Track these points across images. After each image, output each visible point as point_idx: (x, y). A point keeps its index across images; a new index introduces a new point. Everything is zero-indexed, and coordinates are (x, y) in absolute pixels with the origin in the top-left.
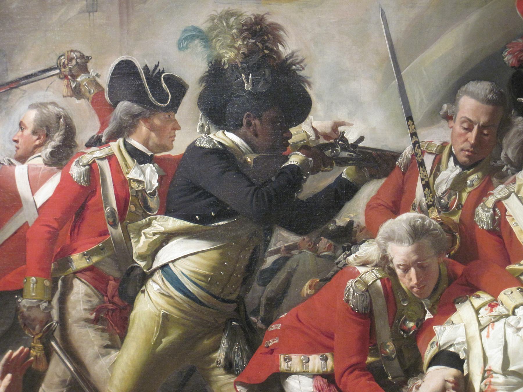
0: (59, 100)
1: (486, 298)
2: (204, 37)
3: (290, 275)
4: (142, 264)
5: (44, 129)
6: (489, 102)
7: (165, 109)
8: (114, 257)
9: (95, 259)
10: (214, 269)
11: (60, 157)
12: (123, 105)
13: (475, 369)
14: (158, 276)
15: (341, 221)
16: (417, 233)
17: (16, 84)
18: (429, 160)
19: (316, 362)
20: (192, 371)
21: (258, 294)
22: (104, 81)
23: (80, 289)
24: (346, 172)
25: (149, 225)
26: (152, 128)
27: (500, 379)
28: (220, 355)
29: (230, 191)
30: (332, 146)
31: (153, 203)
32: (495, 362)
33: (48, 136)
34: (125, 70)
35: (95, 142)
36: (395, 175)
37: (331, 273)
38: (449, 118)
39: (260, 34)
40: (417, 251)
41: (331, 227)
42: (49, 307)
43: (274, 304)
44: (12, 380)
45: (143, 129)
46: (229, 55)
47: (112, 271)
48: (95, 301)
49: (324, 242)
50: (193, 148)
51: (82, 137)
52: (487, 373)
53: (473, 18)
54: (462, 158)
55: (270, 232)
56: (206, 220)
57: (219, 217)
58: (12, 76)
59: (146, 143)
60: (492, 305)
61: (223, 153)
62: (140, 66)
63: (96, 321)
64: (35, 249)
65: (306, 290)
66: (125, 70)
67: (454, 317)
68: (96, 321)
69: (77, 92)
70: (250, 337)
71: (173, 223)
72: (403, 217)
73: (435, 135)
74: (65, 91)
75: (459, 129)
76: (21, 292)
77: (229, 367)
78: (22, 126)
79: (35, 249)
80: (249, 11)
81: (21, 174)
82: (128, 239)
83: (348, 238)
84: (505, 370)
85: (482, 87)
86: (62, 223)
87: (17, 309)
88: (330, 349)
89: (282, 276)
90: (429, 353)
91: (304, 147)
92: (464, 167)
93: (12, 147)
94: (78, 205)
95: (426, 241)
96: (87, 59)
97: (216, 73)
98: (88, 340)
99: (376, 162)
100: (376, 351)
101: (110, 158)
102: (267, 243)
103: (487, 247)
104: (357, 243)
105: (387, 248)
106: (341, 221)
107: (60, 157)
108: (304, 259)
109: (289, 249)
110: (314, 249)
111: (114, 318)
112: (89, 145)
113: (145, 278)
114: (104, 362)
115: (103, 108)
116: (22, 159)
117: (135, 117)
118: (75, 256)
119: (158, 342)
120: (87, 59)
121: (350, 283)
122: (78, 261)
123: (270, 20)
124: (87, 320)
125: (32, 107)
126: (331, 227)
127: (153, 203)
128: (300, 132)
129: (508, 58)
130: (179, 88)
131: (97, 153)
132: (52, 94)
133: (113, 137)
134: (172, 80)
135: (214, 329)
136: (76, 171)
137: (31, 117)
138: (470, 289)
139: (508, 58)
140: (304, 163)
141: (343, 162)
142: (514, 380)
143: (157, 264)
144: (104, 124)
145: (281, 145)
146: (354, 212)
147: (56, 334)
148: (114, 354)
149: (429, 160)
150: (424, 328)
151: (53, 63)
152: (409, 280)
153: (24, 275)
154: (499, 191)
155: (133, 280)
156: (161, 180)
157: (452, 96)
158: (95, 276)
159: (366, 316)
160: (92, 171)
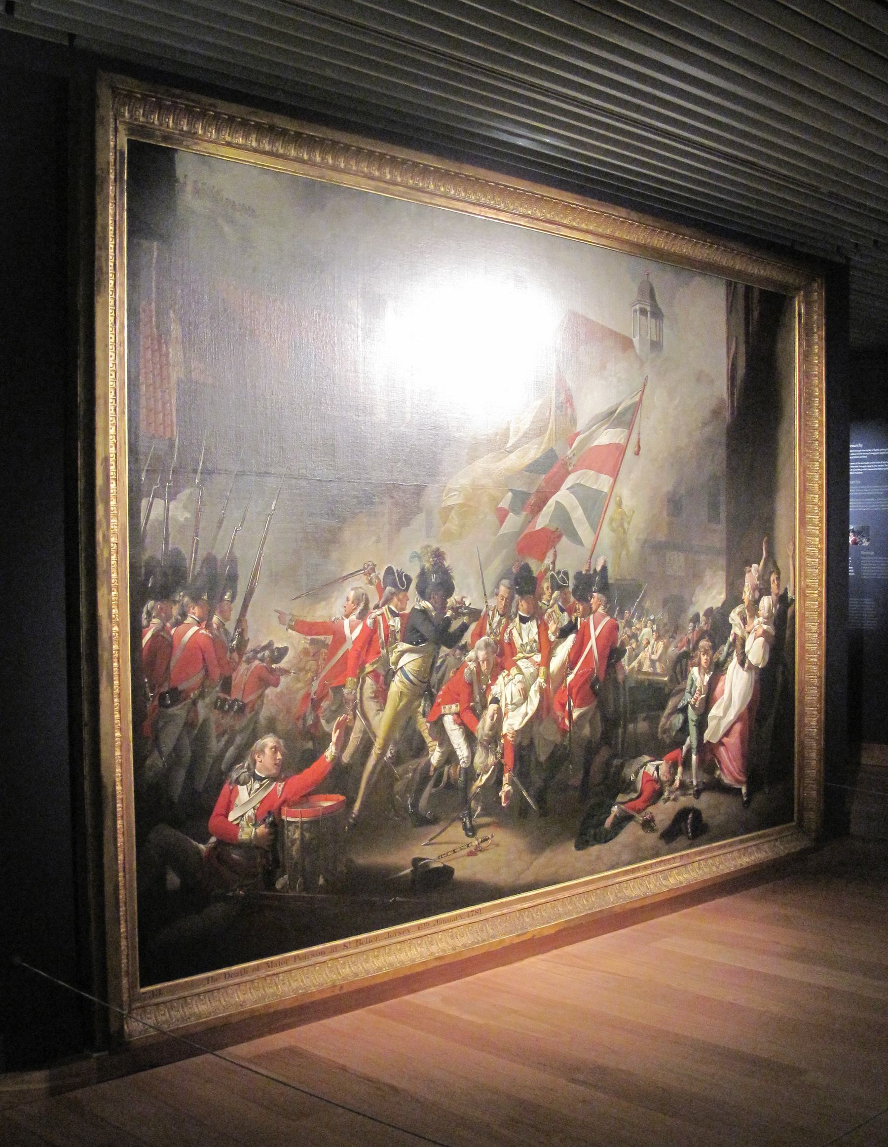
0: (363, 585)
1: (506, 672)
2: (420, 558)
3: (446, 668)
4: (393, 667)
5: (357, 601)
6: (509, 588)
7: (404, 591)
8: (383, 665)
9: (375, 666)
10: (420, 667)
11: (363, 616)
12: (388, 588)
13: (503, 703)
14: (399, 673)
15: (463, 642)
16: (487, 645)
17: (346, 578)
18: (491, 613)
19: (454, 708)
20: (410, 718)
21: (435, 678)
22: (381, 577)
23: (369, 681)
24: (465, 619)
25: (396, 647)
26: (399, 600)
27: (510, 707)
28: (421, 709)
29: (426, 630)
30: (461, 607)
31: (398, 636)
32: (509, 701)
33: (358, 604)
34: (389, 571)
35: (377, 607)
36: (481, 620)
37: (460, 666)
38: (497, 595)
39: (438, 555)
40: (487, 653)
41: (460, 644)
42: (356, 693)
43: (440, 682)
44: (340, 733)
45: (395, 599)
46: (427, 565)
47: (382, 672)
48: (375, 687)
49: (458, 651)
50: (413, 609)
51: (371, 605)
52: (506, 704)
53: (504, 551)
54: (501, 613)
55: (439, 648)
56: (418, 644)
57: (422, 643)
58: (345, 574)
59: (396, 607)
60: (508, 675)
61: (424, 611)
62: (395, 570)
63: (375, 697)
64: (351, 662)
65: (451, 674)
66: (389, 571)
67: (497, 682)
68: (375, 697)
69: (371, 582)
70: (432, 697)
71: (406, 646)
72: (483, 638)
73: (492, 602)
74: (366, 581)
75: (500, 598)
76: (344, 686)
77: (424, 715)
78: (348, 599)
79: (351, 662)
80: (435, 546)
81: (346, 623)
82: (388, 655)
83: (465, 649)
84: (512, 704)
85: (505, 582)
86: (362, 648)
87: (343, 695)
88: (458, 701)
89: (443, 668)
90: (490, 698)
91: (452, 609)
92: (501, 616)
93: (343, 610)
94: (369, 638)
95: (490, 649)
96: (375, 566)
97: (423, 574)
98: (371, 706)
99: (475, 614)
100: (473, 700)
101: (382, 614)
102: (438, 653)
103: (507, 650)
104: (468, 651)
105: (477, 654)
106: (463, 642)
107: (363, 616)
108: (451, 660)
109: (446, 655)
110: (454, 655)
111: (381, 695)
112: (374, 609)
113: (394, 673)
114: (377, 718)
115: (381, 591)
116: (347, 616)
117: (393, 594)
118: (367, 665)
119: (398, 706)
120: (375, 566)
121: (466, 670)
122: (369, 668)
123: (442, 550)
124: (371, 698)
125: (352, 589)
126: (460, 644)
127: (398, 636)
128: (451, 601)
129: (514, 570)
130: (409, 580)
131: (378, 612)
132: (360, 583)
133: (384, 605)
134: (406, 576)
135: (421, 696)
136: (369, 622)
137: (352, 594)
138: (503, 669)
139: (514, 570)
140: (452, 615)
141: (464, 614)
142: (514, 706)
143: (399, 666)
144: (380, 598)
145: (443, 608)
146: (467, 638)
147: (358, 705)
148: (381, 713)
149: (491, 613)
150: (489, 687)
151: (362, 568)
152: (484, 667)
153: (346, 676)
154: (511, 626)
155: (390, 675)
156: (401, 625)
157: (498, 587)
158: (375, 674)
159: (471, 684)
160: (375, 621)
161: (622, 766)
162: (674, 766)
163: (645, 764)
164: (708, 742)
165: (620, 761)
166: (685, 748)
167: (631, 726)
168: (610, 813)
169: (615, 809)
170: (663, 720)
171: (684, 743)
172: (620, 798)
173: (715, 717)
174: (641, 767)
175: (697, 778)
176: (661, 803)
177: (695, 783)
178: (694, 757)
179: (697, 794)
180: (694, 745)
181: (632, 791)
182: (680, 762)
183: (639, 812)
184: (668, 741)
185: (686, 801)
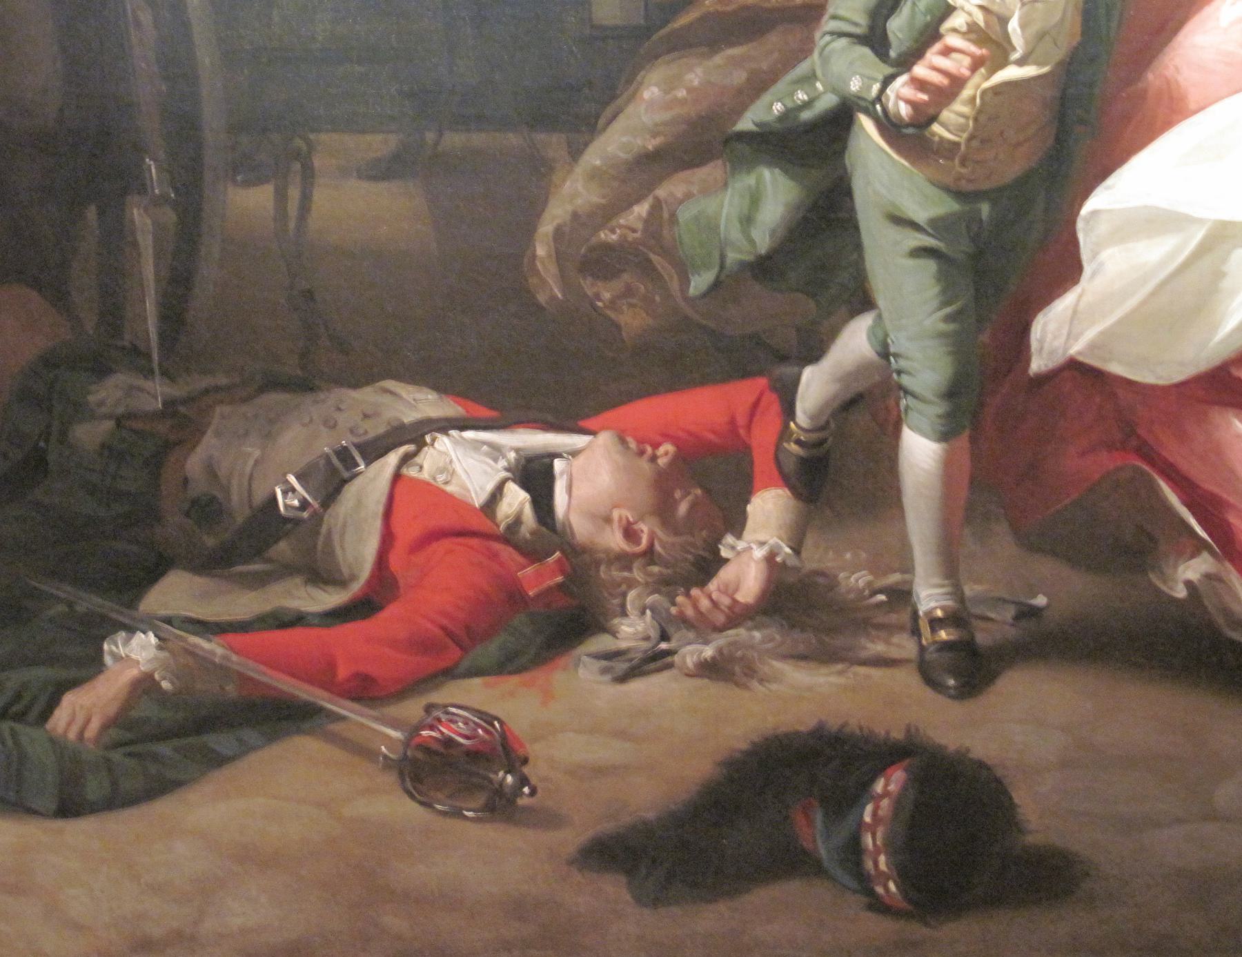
161: (182, 422)
162: (707, 484)
163: (415, 435)
164: (1077, 371)
165: (155, 393)
166: (815, 386)
167: (249, 203)
168: (93, 664)
169: (136, 652)
170: (573, 193)
171: (813, 352)
172: (175, 593)
173: (1156, 222)
174: (374, 450)
175: (950, 568)
176: (581, 677)
177: (930, 597)
178: (920, 451)
179: (969, 665)
180: (926, 370)
181: (287, 570)
182: (762, 461)
183: (365, 690)
184: (632, 320)
185: (802, 692)
